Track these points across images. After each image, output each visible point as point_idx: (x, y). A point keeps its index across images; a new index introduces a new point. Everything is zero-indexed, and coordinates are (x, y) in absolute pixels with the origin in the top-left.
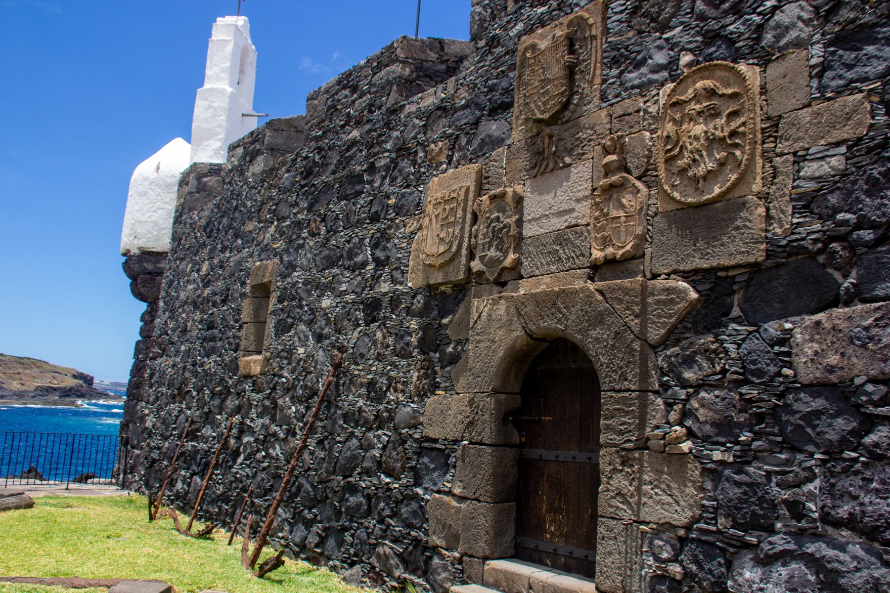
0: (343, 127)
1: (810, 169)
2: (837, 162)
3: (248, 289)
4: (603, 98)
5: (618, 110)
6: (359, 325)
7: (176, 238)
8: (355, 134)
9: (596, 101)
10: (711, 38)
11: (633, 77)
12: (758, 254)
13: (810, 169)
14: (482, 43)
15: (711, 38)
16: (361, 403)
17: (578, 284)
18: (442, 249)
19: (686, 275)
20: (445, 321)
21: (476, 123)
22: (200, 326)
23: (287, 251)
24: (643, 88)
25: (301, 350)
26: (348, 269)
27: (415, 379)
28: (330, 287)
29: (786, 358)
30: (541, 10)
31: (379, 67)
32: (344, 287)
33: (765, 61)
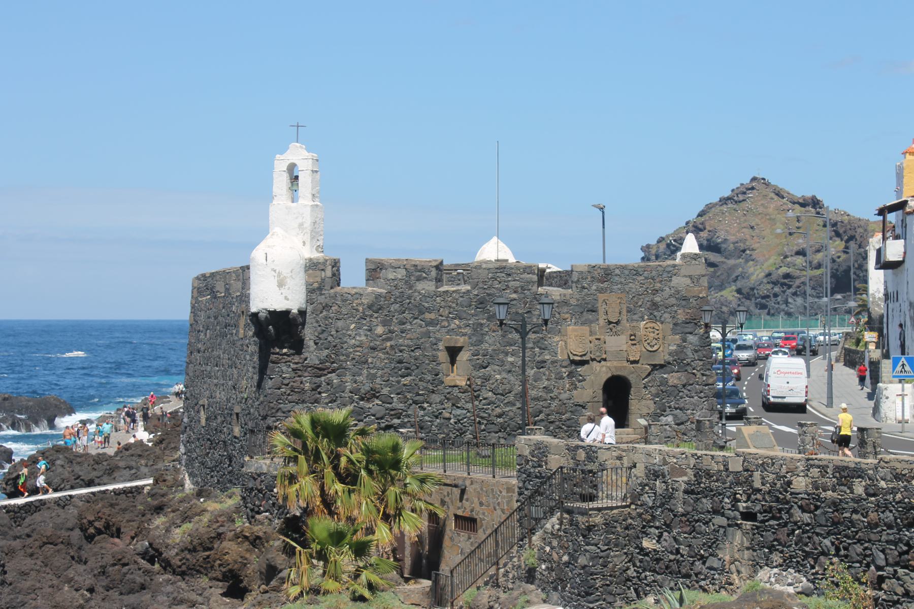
0: (504, 290)
1: (671, 348)
2: (675, 348)
3: (441, 347)
4: (628, 321)
5: (632, 325)
6: (533, 368)
7: (309, 301)
8: (514, 296)
10: (651, 314)
11: (635, 317)
12: (662, 362)
14: (580, 286)
15: (651, 314)
16: (540, 394)
17: (625, 365)
18: (581, 350)
20: (579, 370)
21: (582, 313)
22: (385, 361)
23: (473, 335)
24: (637, 321)
25: (498, 377)
27: (567, 386)
29: (667, 382)
31: (524, 272)
33: (662, 323)
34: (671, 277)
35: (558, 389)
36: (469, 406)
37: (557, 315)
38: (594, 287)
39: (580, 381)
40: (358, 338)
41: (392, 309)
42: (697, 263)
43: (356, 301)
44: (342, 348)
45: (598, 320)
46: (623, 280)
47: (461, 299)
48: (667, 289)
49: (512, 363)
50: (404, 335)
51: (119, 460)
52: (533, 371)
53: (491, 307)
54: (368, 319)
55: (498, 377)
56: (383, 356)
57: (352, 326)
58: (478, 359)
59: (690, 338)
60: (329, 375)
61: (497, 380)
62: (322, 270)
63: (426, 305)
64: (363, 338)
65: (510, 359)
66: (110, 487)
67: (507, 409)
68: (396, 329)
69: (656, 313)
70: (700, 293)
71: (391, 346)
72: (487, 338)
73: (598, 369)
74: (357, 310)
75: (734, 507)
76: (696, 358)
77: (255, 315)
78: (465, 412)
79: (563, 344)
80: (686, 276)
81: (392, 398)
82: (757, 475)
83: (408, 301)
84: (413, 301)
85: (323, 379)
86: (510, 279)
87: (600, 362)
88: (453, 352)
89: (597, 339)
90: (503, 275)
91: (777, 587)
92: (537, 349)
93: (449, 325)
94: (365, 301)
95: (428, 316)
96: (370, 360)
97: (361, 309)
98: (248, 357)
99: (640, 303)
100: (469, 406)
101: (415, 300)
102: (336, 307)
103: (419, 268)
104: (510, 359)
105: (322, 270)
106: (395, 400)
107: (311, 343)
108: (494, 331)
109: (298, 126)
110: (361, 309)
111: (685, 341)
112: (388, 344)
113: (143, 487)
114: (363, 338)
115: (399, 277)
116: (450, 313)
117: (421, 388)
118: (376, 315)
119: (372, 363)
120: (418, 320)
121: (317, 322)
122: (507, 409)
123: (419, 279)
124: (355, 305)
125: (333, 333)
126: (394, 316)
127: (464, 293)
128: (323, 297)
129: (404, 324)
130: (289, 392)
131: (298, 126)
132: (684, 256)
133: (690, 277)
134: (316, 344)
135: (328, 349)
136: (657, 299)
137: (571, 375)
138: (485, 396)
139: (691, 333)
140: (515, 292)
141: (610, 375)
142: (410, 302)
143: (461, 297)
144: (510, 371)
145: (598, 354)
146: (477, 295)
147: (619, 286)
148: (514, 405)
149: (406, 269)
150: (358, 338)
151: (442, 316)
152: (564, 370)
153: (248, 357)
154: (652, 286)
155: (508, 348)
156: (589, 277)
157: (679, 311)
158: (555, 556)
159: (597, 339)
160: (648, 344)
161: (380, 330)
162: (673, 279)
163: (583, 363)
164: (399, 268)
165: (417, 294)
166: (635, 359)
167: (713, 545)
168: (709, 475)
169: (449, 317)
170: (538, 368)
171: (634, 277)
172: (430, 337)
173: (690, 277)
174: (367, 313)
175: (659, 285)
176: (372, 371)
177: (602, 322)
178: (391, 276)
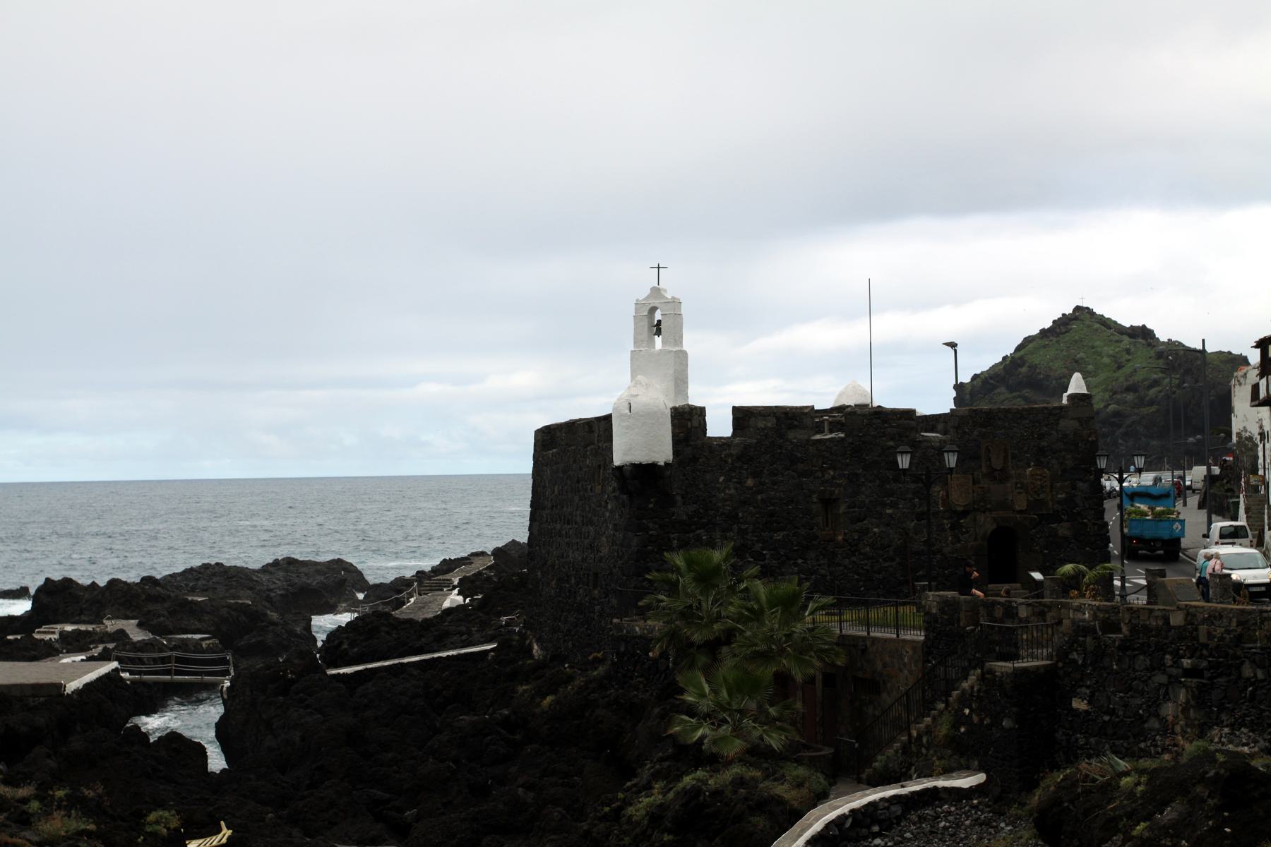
1: (1059, 496)
2: (1063, 496)
3: (815, 500)
4: (1013, 467)
6: (913, 521)
9: (1010, 468)
13: (1059, 496)
16: (922, 548)
19: (1037, 515)
20: (962, 521)
22: (757, 516)
25: (876, 530)
26: (901, 499)
27: (950, 538)
28: (892, 506)
30: (984, 430)
31: (901, 418)
32: (901, 506)
33: (1049, 470)
34: (1058, 420)
35: (940, 542)
36: (846, 562)
37: (938, 464)
38: (976, 433)
39: (963, 533)
40: (727, 492)
41: (763, 460)
42: (1086, 404)
43: (724, 452)
44: (711, 502)
45: (981, 467)
46: (1007, 424)
47: (835, 448)
48: (1054, 432)
49: (890, 515)
50: (776, 487)
51: (448, 626)
52: (913, 524)
53: (867, 455)
54: (738, 471)
55: (876, 530)
56: (754, 511)
57: (721, 479)
58: (854, 512)
59: (1080, 484)
60: (698, 531)
61: (875, 534)
62: (688, 420)
63: (799, 455)
64: (732, 491)
65: (889, 511)
66: (444, 654)
67: (886, 564)
68: (767, 481)
69: (1042, 459)
70: (1090, 435)
71: (762, 500)
72: (864, 489)
73: (982, 519)
74: (726, 462)
75: (1176, 663)
76: (1087, 506)
77: (620, 468)
78: (841, 568)
79: (945, 494)
80: (1073, 419)
81: (764, 555)
82: (1203, 629)
83: (779, 451)
84: (784, 451)
85: (691, 535)
86: (886, 425)
87: (984, 512)
88: (828, 503)
89: (980, 488)
90: (879, 421)
91: (1231, 747)
92: (917, 500)
93: (823, 476)
94: (734, 451)
95: (800, 466)
96: (740, 515)
97: (730, 460)
98: (607, 514)
99: (1025, 449)
100: (846, 562)
101: (786, 450)
102: (704, 459)
103: (790, 415)
104: (889, 511)
105: (688, 420)
106: (767, 556)
107: (679, 498)
108: (870, 481)
109: (659, 268)
110: (730, 460)
111: (1074, 488)
112: (759, 497)
113: (487, 652)
114: (732, 491)
115: (769, 425)
116: (824, 463)
117: (795, 543)
118: (745, 466)
119: (742, 518)
120: (790, 472)
121: (684, 475)
122: (886, 564)
123: (791, 427)
124: (723, 456)
125: (701, 486)
126: (764, 468)
127: (838, 441)
128: (690, 448)
129: (776, 475)
130: (656, 550)
131: (659, 268)
132: (1071, 397)
133: (1079, 419)
134: (683, 498)
135: (696, 503)
136: (1044, 444)
137: (952, 528)
138: (863, 551)
139: (1080, 480)
140: (892, 439)
141: (994, 526)
142: (781, 453)
143: (836, 446)
144: (888, 525)
145: (982, 504)
146: (852, 443)
147: (1003, 431)
148: (893, 560)
149: (776, 417)
150: (727, 492)
151: (816, 467)
152: (945, 521)
153: (607, 514)
154: (1037, 430)
155: (886, 499)
156: (970, 421)
157: (1068, 456)
158: (975, 719)
159: (980, 488)
160: (1035, 492)
161: (750, 482)
162: (1060, 422)
163: (965, 513)
164: (769, 416)
165: (788, 443)
166: (1021, 508)
167: (1154, 706)
168: (1146, 629)
169: (823, 467)
170: (918, 520)
171: (1019, 421)
172: (803, 489)
173: (1079, 419)
174: (736, 465)
175: (1045, 429)
176: (743, 527)
177: (984, 470)
178: (761, 425)
